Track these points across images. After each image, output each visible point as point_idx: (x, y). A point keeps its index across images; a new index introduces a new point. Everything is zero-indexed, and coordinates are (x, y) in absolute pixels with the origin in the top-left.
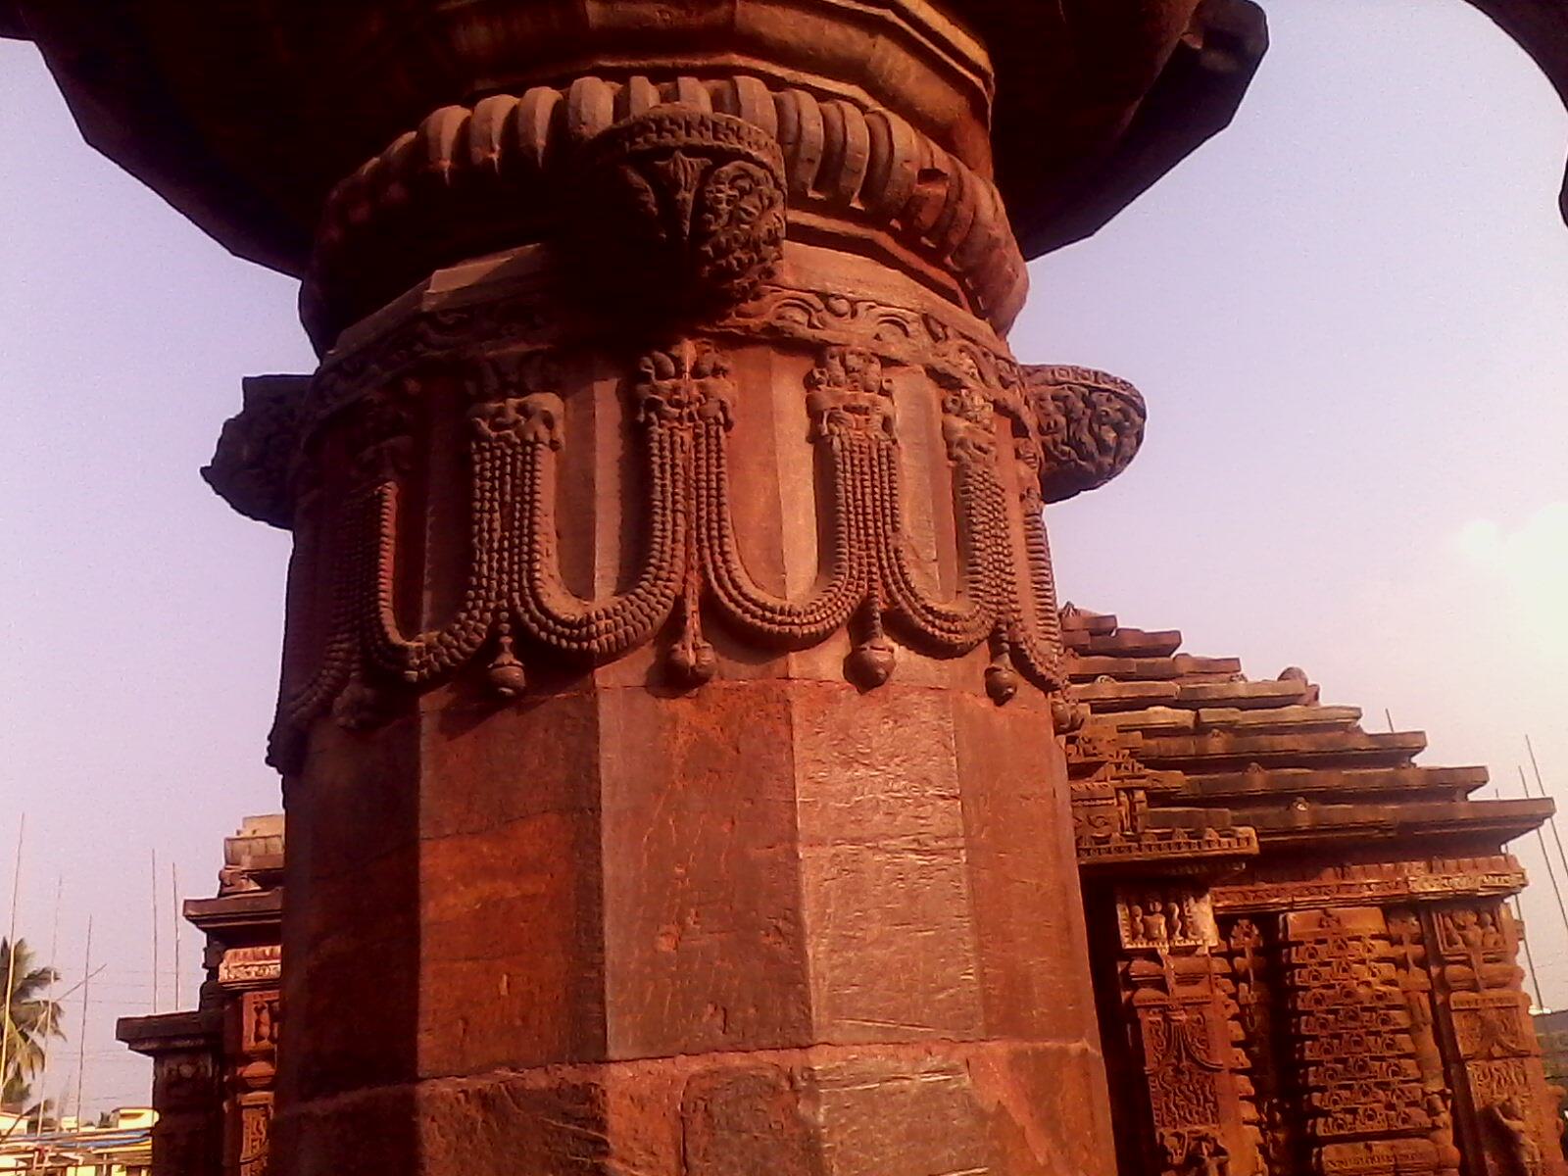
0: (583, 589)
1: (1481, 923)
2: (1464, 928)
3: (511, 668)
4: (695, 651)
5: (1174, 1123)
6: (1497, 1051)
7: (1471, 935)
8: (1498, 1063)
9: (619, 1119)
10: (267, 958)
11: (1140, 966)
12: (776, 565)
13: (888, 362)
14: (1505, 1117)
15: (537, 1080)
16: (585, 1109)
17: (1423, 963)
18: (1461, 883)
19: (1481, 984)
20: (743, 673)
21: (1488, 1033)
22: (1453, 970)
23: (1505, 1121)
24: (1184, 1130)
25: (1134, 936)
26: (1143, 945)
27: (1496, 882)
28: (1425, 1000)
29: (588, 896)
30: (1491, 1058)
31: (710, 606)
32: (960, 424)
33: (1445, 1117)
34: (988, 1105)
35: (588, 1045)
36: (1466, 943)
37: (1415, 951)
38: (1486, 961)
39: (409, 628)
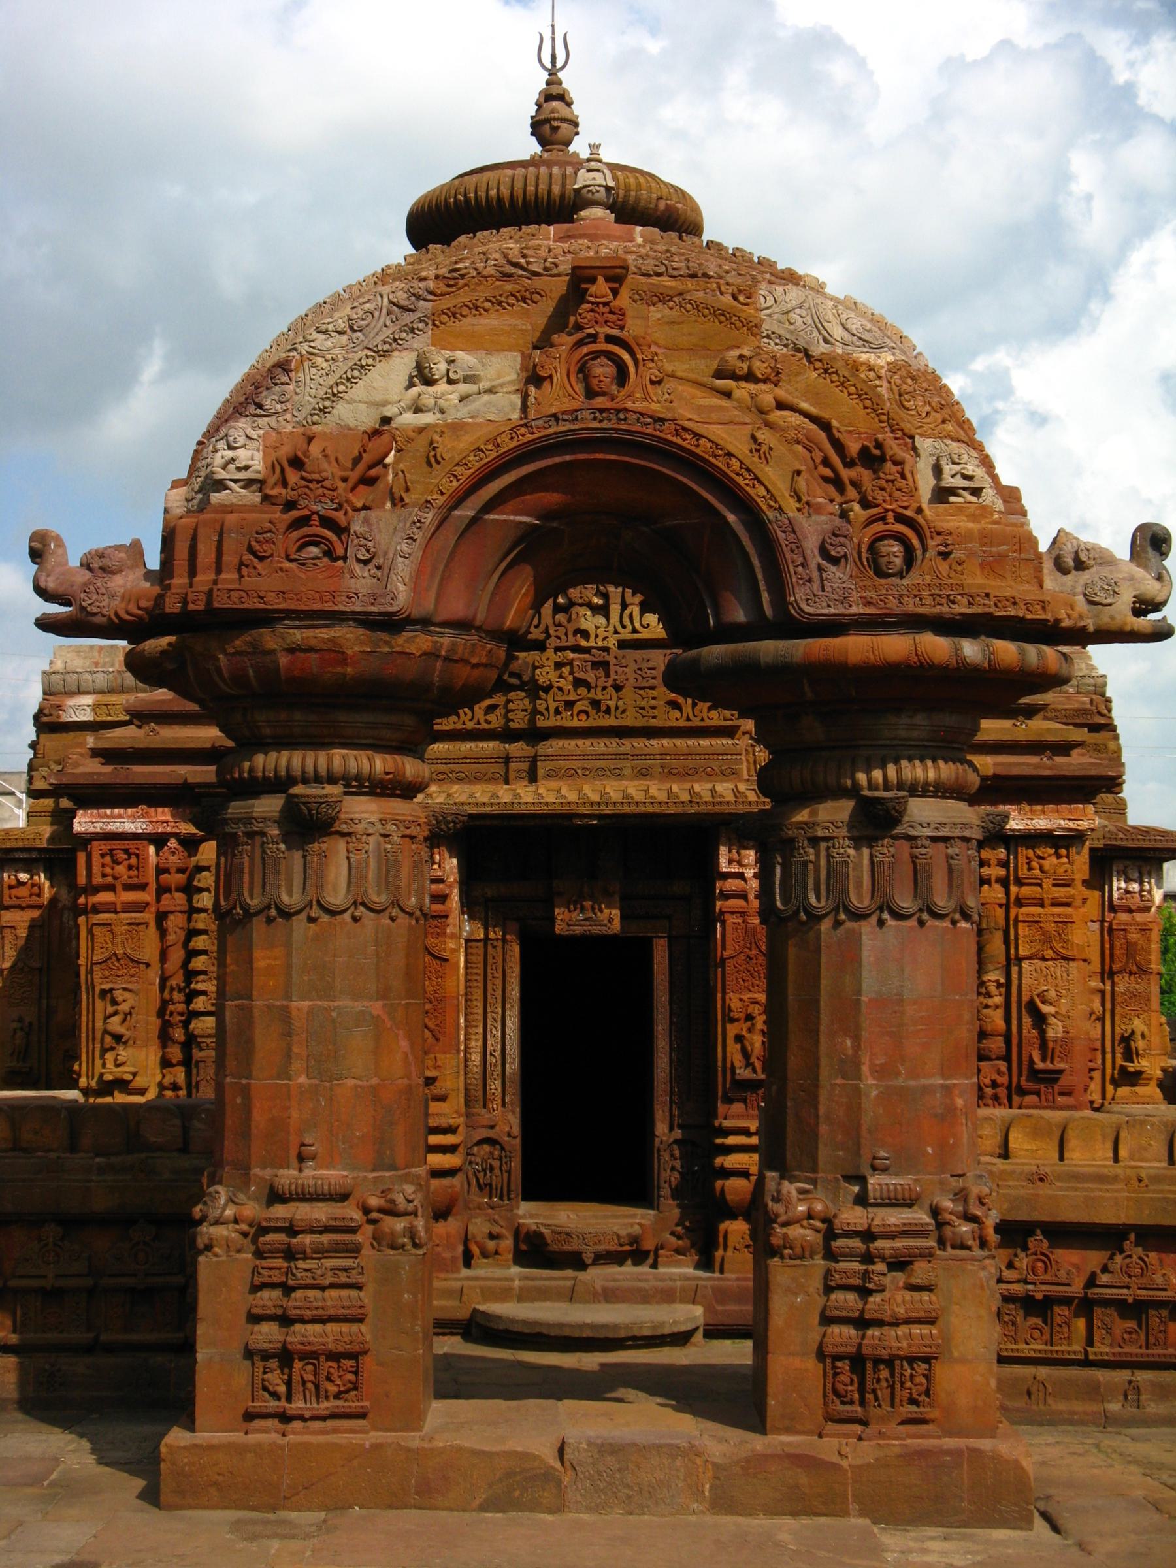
0: (290, 894)
1: (1059, 857)
2: (1043, 858)
3: (273, 912)
4: (315, 912)
5: (740, 991)
6: (1049, 953)
7: (1046, 864)
8: (1050, 963)
9: (294, 1013)
10: (108, 817)
11: (732, 884)
12: (335, 890)
13: (368, 835)
14: (1043, 1003)
15: (278, 1003)
16: (286, 1010)
17: (1004, 882)
18: (1041, 823)
19: (1047, 902)
20: (326, 918)
21: (1047, 940)
22: (1026, 891)
23: (1041, 1006)
24: (744, 997)
25: (730, 862)
26: (734, 869)
27: (1072, 825)
28: (1000, 913)
29: (289, 966)
30: (1044, 959)
31: (318, 902)
32: (389, 846)
33: (998, 1000)
34: (375, 1013)
35: (288, 997)
36: (1042, 870)
37: (997, 872)
38: (1054, 885)
39: (252, 897)
